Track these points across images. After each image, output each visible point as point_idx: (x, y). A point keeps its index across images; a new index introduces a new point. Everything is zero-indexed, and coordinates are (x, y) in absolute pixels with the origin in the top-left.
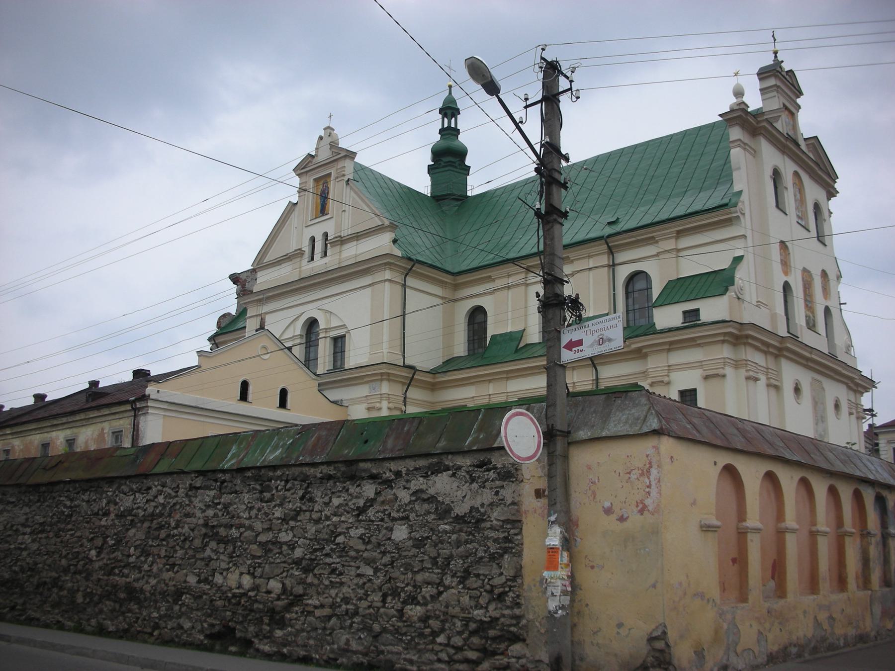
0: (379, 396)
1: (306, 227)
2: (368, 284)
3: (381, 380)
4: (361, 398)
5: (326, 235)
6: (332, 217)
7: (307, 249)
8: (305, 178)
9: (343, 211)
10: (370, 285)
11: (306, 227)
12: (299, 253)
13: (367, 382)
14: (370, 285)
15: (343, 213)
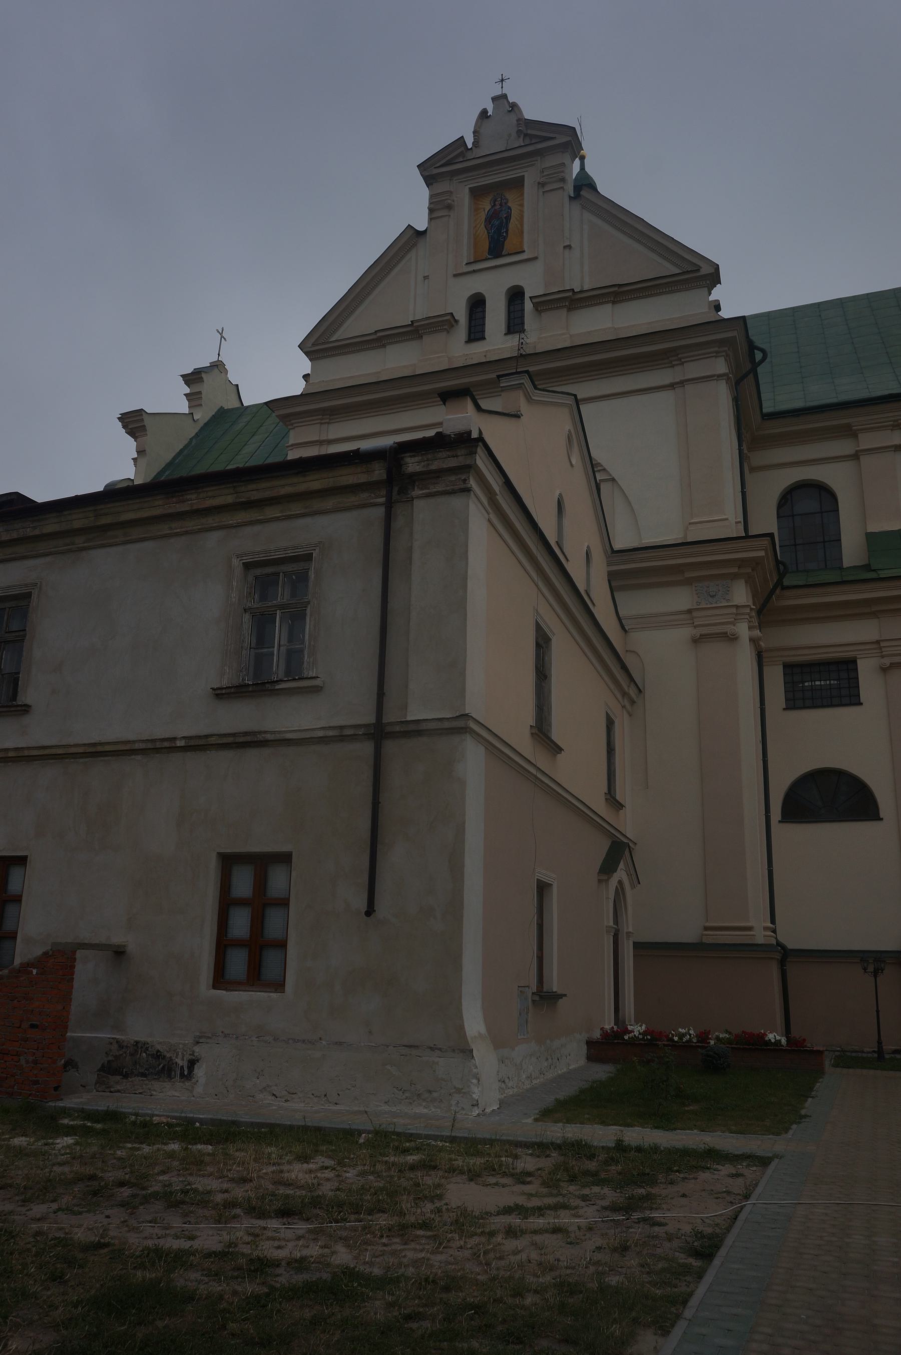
0: (734, 610)
1: (455, 276)
2: (667, 382)
3: (735, 577)
4: (672, 614)
5: (516, 295)
6: (536, 258)
7: (462, 315)
8: (442, 187)
9: (565, 247)
10: (672, 386)
11: (455, 276)
12: (446, 323)
13: (689, 582)
14: (672, 386)
15: (567, 251)
